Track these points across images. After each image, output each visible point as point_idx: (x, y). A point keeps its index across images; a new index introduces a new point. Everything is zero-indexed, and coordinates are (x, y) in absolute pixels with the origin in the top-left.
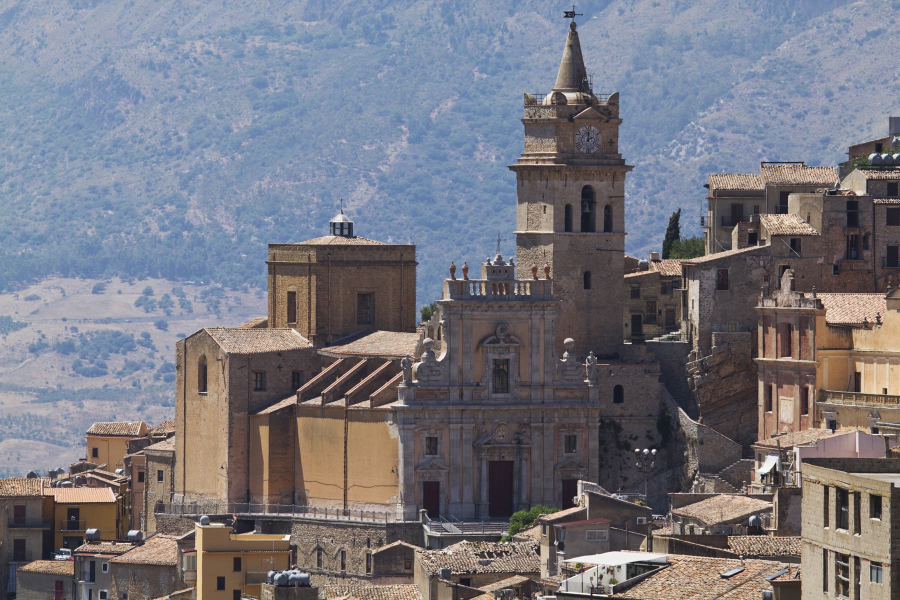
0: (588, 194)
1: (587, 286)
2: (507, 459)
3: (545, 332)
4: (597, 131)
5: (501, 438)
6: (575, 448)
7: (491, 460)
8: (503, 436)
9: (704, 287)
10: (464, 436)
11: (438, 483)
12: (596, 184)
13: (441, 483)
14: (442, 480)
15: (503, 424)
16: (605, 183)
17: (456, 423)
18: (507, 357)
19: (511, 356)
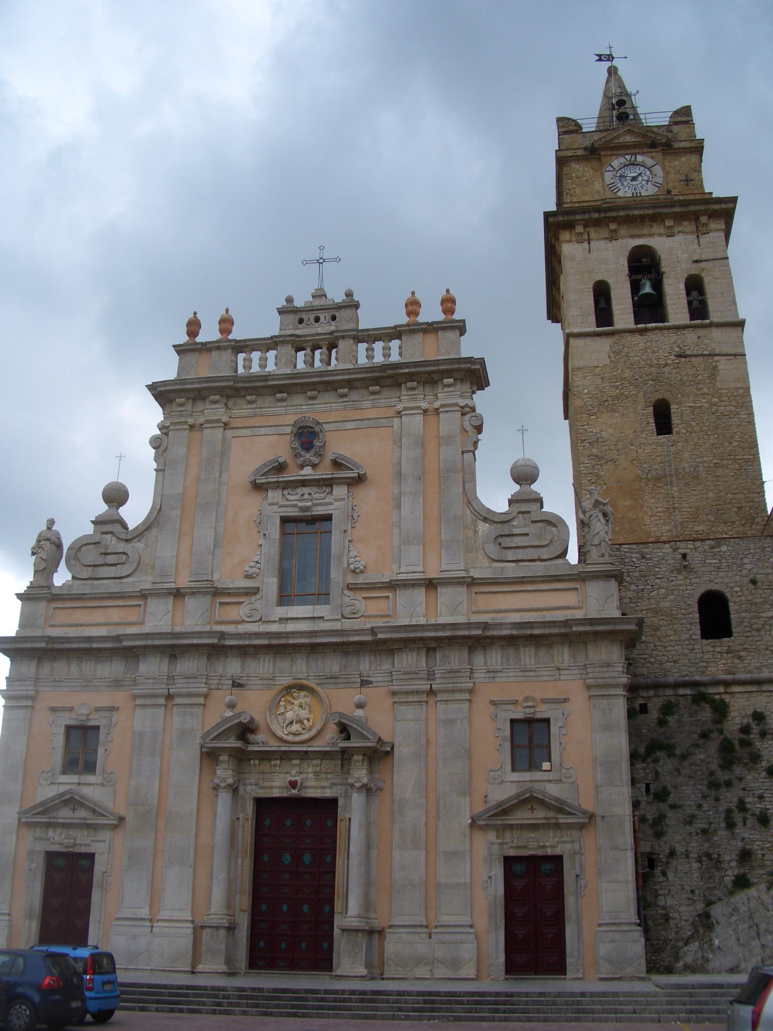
5: (296, 727)
8: (300, 721)
13: (97, 857)
16: (678, 238)
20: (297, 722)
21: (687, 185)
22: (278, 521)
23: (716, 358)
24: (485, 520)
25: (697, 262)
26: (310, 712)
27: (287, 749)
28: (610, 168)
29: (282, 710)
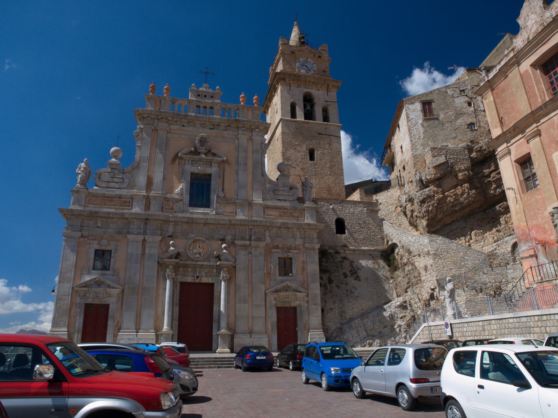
0: (308, 100)
1: (312, 158)
2: (205, 280)
3: (254, 152)
4: (312, 62)
5: (197, 256)
6: (292, 273)
7: (183, 280)
8: (200, 254)
9: (410, 117)
10: (147, 251)
11: (107, 307)
12: (314, 92)
13: (111, 306)
14: (112, 302)
15: (200, 240)
16: (321, 92)
17: (138, 234)
18: (208, 170)
19: (213, 170)
20: (198, 253)
21: (324, 73)
22: (190, 174)
23: (331, 137)
24: (269, 183)
25: (326, 101)
26: (203, 249)
27: (195, 263)
28: (298, 61)
29: (192, 248)
